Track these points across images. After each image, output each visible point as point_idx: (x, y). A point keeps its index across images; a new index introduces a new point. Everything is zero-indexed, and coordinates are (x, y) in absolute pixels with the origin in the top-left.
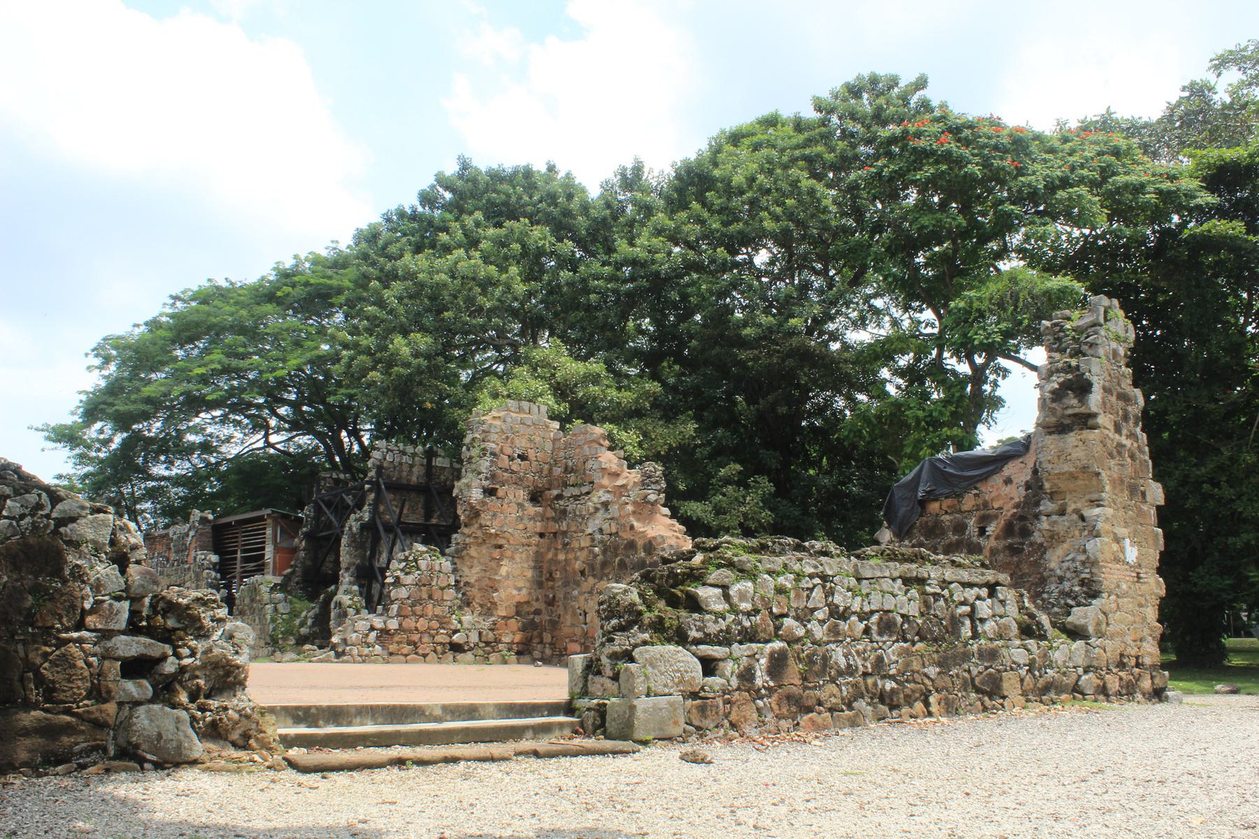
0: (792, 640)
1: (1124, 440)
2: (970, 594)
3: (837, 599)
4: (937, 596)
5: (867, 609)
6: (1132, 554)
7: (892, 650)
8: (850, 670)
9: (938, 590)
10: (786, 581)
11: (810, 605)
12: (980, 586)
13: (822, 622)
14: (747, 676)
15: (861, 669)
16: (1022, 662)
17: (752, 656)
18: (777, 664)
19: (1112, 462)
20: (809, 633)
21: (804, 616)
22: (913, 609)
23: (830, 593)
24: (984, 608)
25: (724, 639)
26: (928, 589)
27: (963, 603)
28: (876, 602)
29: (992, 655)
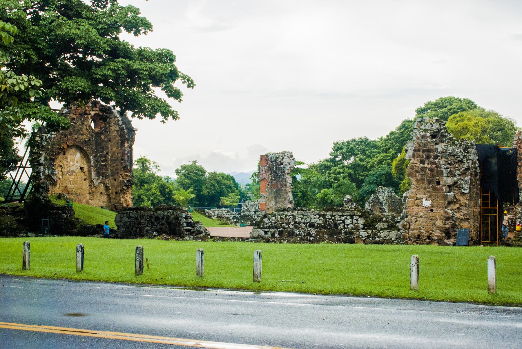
0: (284, 228)
1: (426, 165)
2: (343, 218)
3: (296, 220)
4: (329, 219)
5: (306, 222)
6: (427, 203)
7: (313, 232)
8: (300, 235)
9: (330, 217)
10: (283, 217)
11: (289, 221)
12: (347, 216)
13: (293, 225)
14: (273, 235)
15: (303, 235)
16: (364, 235)
17: (275, 231)
18: (280, 233)
19: (418, 174)
20: (289, 227)
21: (288, 223)
22: (321, 222)
23: (295, 218)
24: (348, 222)
25: (269, 228)
26: (326, 217)
27: (341, 220)
28: (308, 220)
29: (351, 233)
